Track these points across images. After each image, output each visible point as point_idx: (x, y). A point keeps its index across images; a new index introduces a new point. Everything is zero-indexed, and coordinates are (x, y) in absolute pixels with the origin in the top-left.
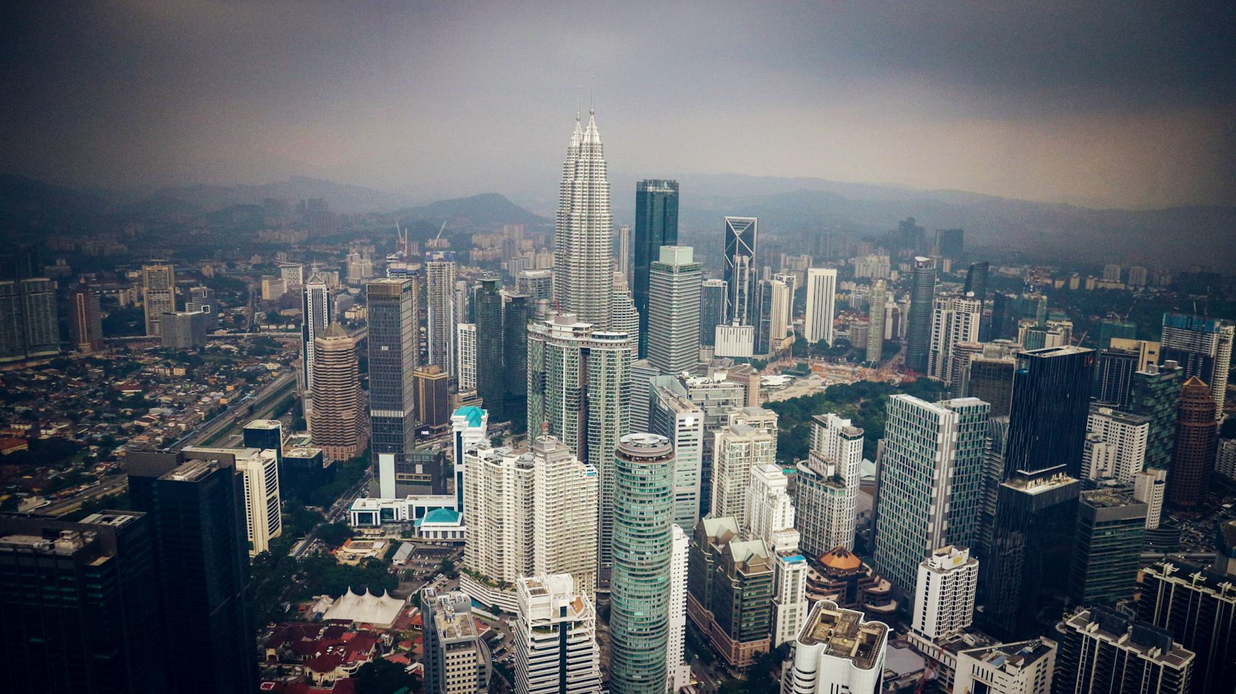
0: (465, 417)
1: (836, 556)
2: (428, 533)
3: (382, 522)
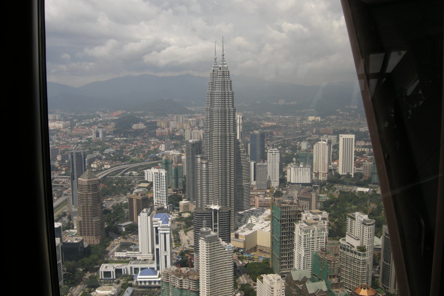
0: (159, 219)
1: (363, 289)
2: (141, 282)
3: (116, 276)
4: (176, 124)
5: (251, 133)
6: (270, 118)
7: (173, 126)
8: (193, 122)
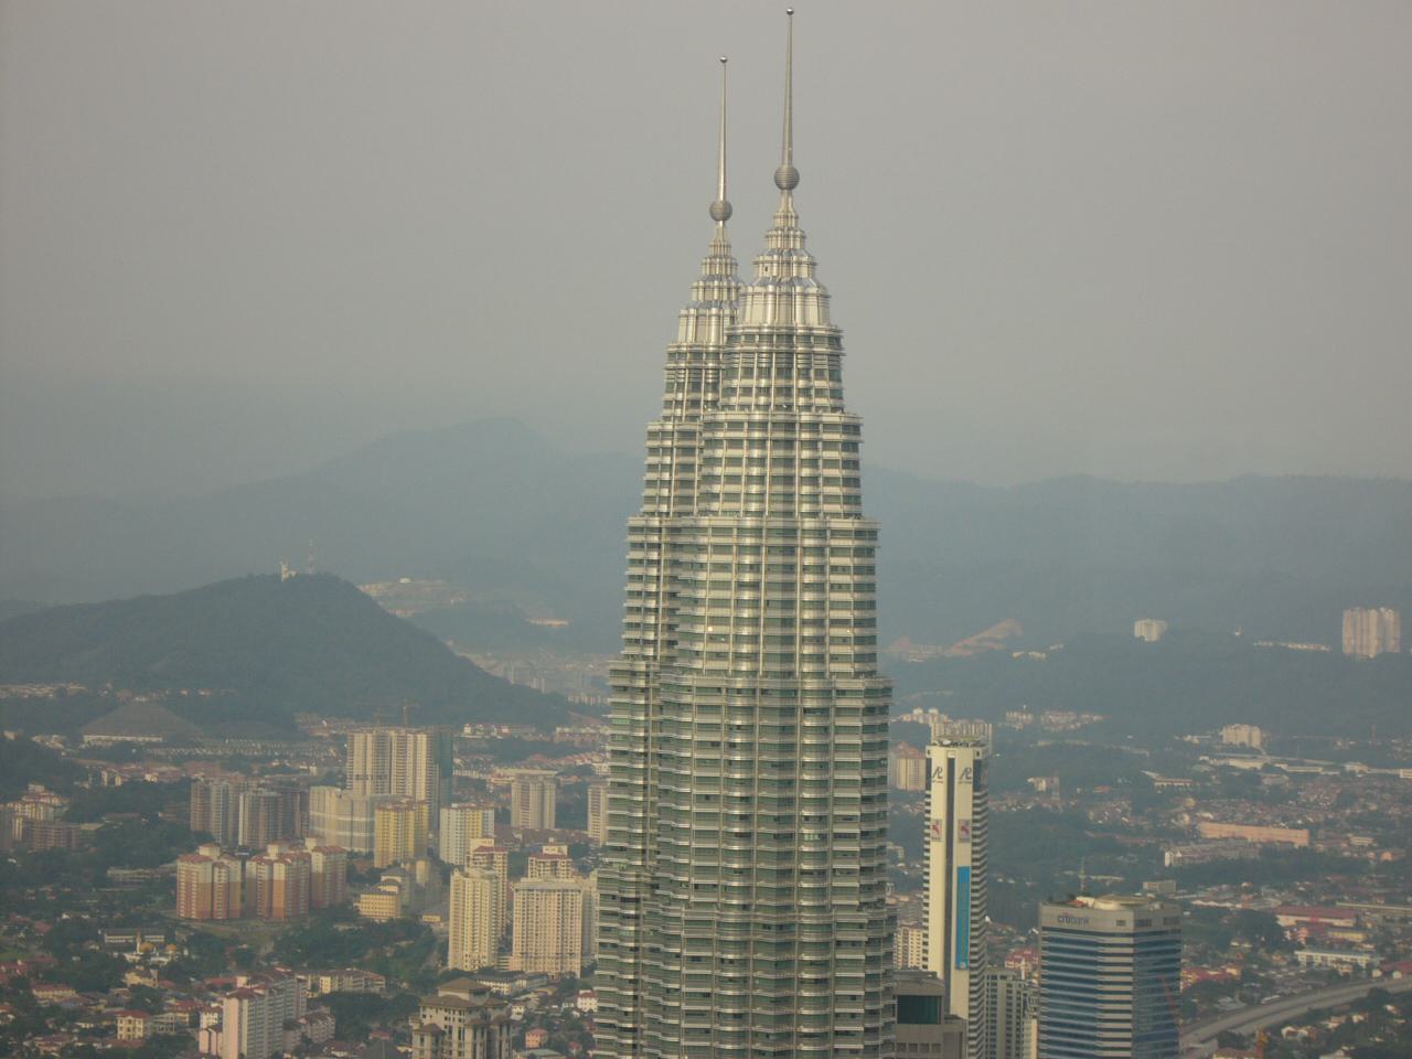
4: (373, 806)
5: (1050, 914)
6: (1252, 777)
7: (341, 826)
8: (534, 796)
